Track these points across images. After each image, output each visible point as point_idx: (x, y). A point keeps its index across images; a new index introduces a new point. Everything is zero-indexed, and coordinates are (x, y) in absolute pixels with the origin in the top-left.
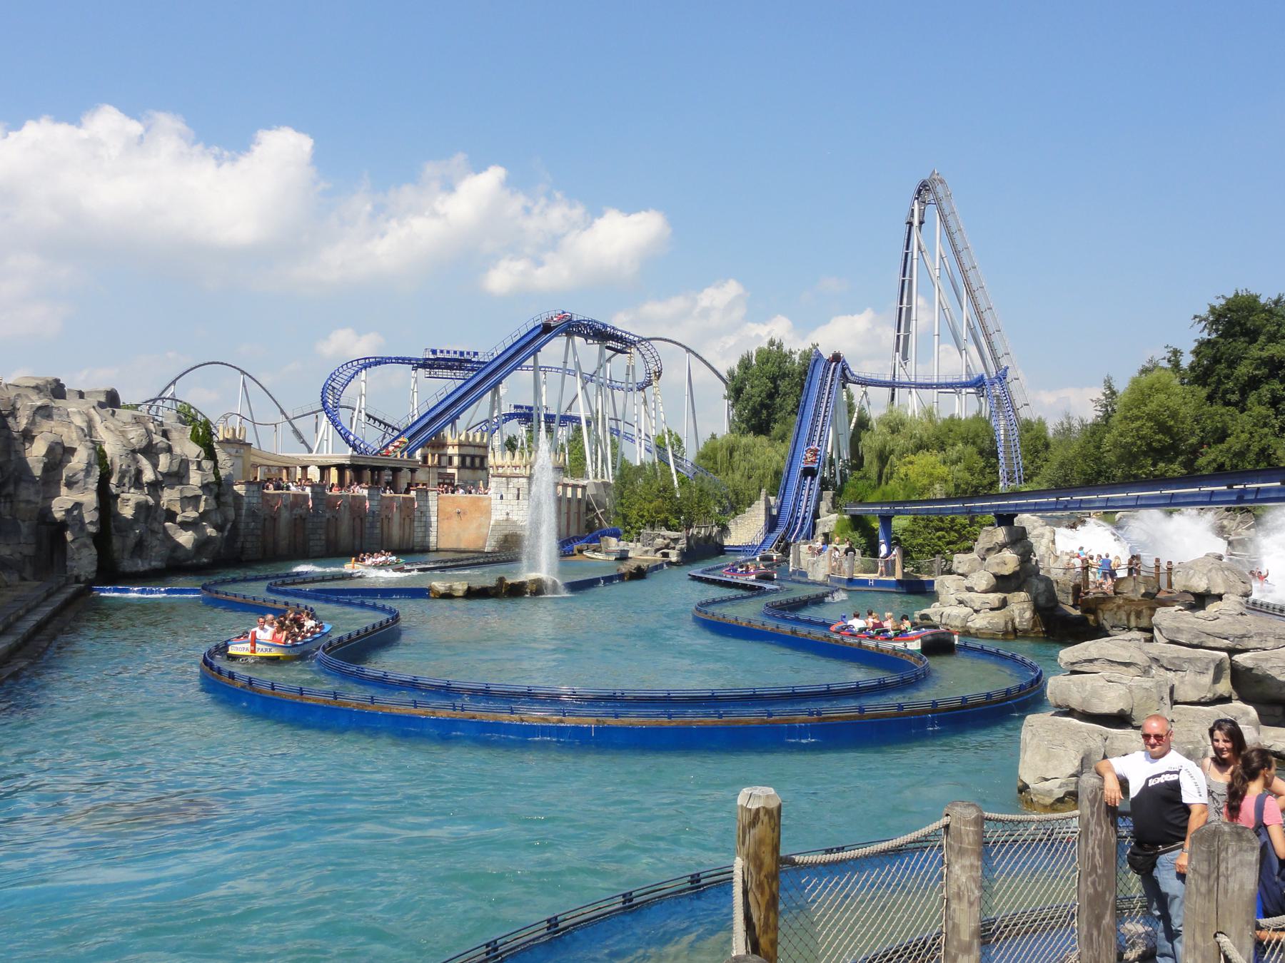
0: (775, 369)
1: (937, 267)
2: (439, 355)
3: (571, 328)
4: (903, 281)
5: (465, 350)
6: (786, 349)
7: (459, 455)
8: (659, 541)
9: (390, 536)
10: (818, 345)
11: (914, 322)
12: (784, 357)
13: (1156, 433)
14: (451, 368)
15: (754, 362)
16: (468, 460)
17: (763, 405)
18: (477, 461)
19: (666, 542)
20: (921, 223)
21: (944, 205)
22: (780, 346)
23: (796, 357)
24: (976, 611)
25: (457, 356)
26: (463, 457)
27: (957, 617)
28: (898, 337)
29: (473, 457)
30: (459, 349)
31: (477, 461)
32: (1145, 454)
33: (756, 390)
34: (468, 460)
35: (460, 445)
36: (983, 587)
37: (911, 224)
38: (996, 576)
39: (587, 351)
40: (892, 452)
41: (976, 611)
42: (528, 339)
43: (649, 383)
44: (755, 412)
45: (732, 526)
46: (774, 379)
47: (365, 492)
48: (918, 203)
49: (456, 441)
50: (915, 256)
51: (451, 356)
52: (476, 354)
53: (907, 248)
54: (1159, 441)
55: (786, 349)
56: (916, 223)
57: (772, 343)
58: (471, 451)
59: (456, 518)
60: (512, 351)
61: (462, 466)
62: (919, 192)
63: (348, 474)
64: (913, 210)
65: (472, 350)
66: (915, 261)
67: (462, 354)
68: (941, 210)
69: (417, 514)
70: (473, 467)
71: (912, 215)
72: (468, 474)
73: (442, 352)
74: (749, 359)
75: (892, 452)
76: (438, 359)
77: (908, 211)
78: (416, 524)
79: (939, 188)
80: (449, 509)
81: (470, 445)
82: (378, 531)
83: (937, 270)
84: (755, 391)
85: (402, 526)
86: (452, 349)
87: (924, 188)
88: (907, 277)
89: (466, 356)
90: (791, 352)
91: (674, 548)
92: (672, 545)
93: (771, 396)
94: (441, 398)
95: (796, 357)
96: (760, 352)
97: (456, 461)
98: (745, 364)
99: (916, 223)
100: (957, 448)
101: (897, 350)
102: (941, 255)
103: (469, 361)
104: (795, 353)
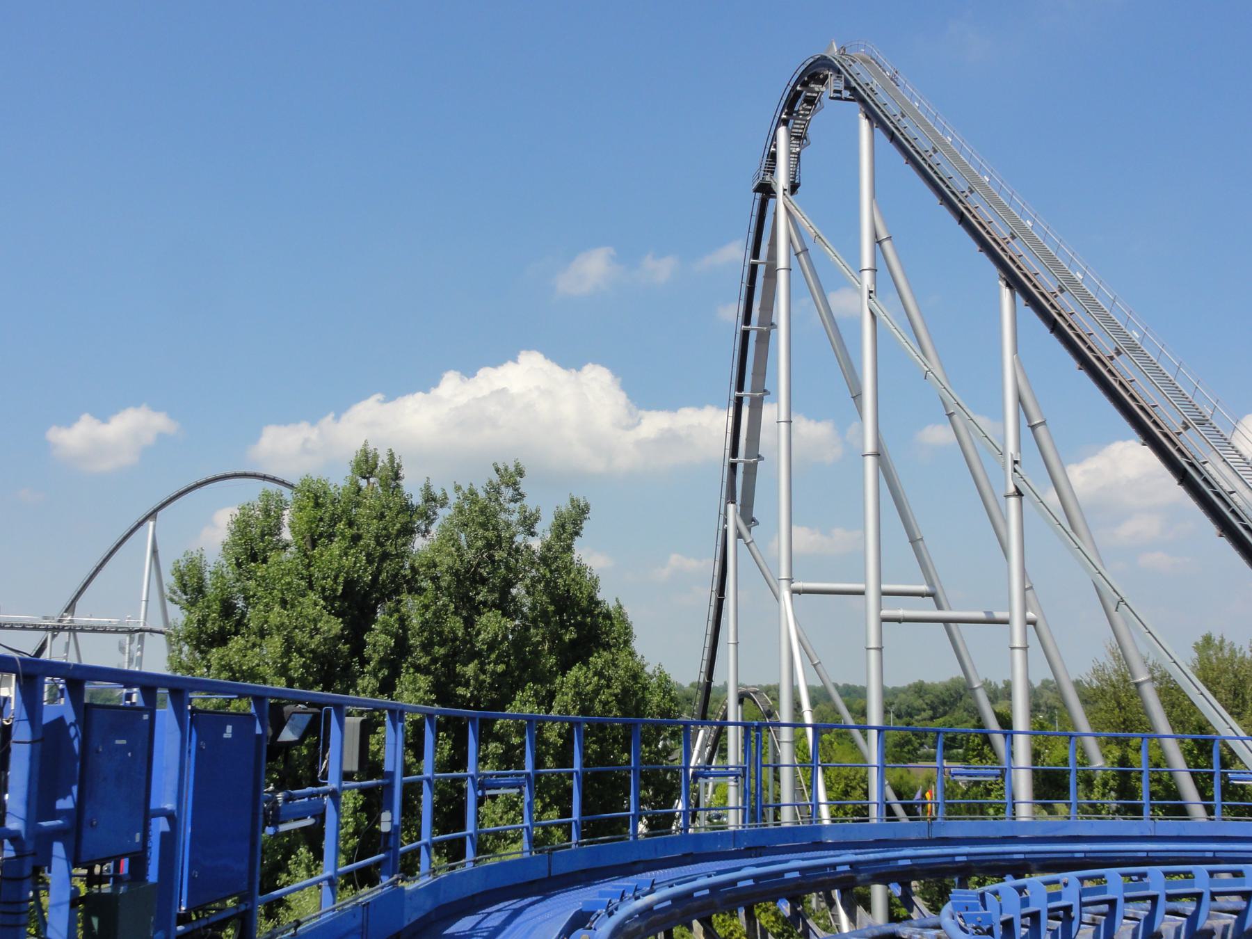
1: (867, 262)
4: (745, 335)
10: (520, 473)
15: (286, 535)
20: (794, 188)
28: (733, 467)
37: (766, 191)
50: (782, 262)
53: (756, 254)
62: (790, 104)
64: (773, 157)
66: (782, 276)
83: (867, 276)
87: (815, 72)
99: (781, 180)
101: (731, 498)
102: (875, 234)
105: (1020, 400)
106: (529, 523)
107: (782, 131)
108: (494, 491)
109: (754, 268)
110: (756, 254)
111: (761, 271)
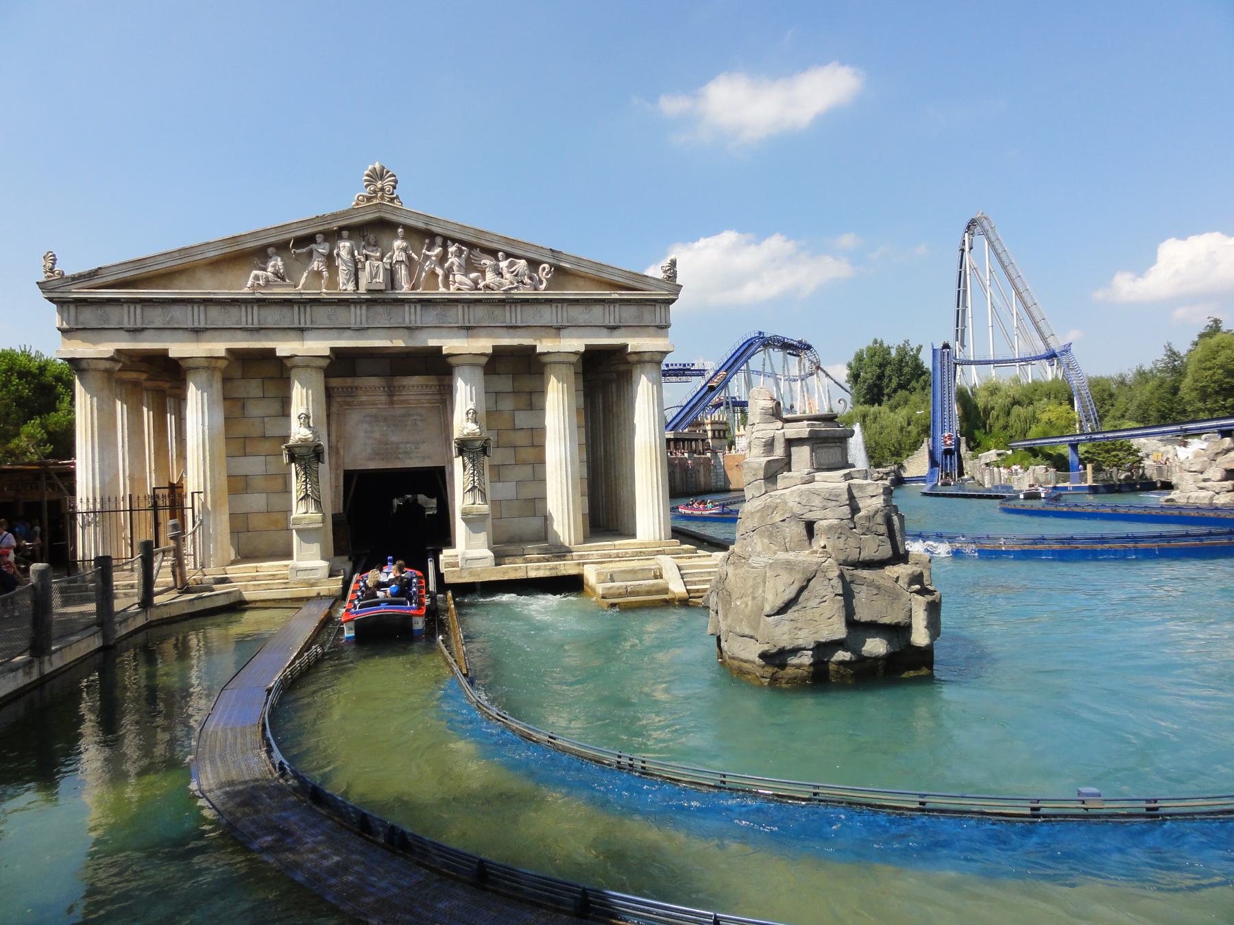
0: (881, 360)
1: (988, 278)
2: (670, 367)
3: (768, 343)
5: (686, 362)
6: (885, 345)
7: (712, 430)
8: (876, 475)
9: (700, 481)
11: (970, 319)
12: (887, 351)
13: (1225, 378)
14: (677, 375)
16: (717, 433)
17: (875, 385)
18: (722, 433)
19: (880, 475)
21: (991, 235)
22: (881, 344)
23: (893, 353)
24: (1218, 493)
25: (682, 367)
26: (713, 431)
27: (1205, 498)
28: (957, 330)
29: (719, 431)
30: (682, 362)
31: (722, 433)
32: (1217, 393)
33: (869, 375)
34: (717, 433)
35: (712, 423)
36: (1219, 478)
37: (963, 250)
38: (1226, 470)
39: (777, 355)
40: (993, 408)
41: (1218, 493)
42: (741, 351)
43: (811, 374)
44: (870, 389)
45: (905, 463)
46: (881, 366)
47: (686, 455)
48: (969, 235)
49: (709, 421)
50: (968, 272)
51: (678, 367)
52: (693, 364)
53: (961, 268)
54: (1227, 383)
55: (885, 345)
56: (967, 249)
57: (876, 342)
58: (717, 427)
59: (736, 469)
60: (732, 360)
61: (714, 437)
62: (968, 227)
63: (672, 444)
65: (691, 362)
66: (968, 277)
67: (684, 365)
68: (988, 239)
69: (712, 467)
70: (720, 438)
71: (964, 244)
72: (717, 442)
73: (672, 365)
74: (862, 352)
75: (993, 408)
76: (670, 370)
77: (960, 241)
78: (712, 474)
79: (985, 223)
80: (731, 464)
81: (716, 423)
82: (694, 479)
83: (988, 282)
84: (867, 375)
85: (705, 476)
86: (678, 363)
87: (971, 225)
88: (962, 288)
89: (687, 367)
90: (889, 347)
91: (886, 479)
92: (885, 477)
93: (880, 377)
94: (694, 394)
95: (893, 353)
96: (869, 348)
97: (710, 434)
98: (859, 358)
99: (967, 249)
100: (1043, 402)
101: (957, 340)
103: (689, 370)
104: (892, 348)
105: (1017, 314)
106: (912, 350)
107: (966, 234)
108: (904, 345)
109: (960, 272)
110: (961, 268)
111: (963, 272)
